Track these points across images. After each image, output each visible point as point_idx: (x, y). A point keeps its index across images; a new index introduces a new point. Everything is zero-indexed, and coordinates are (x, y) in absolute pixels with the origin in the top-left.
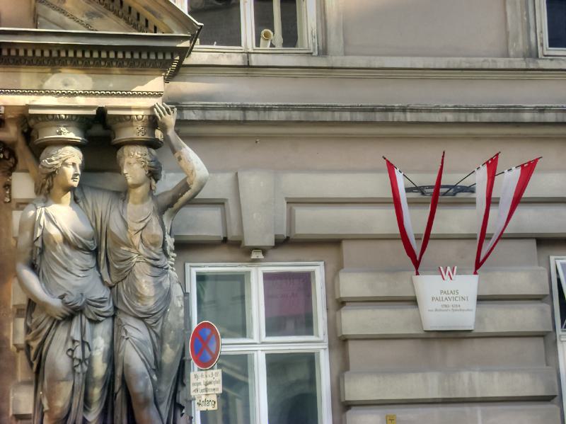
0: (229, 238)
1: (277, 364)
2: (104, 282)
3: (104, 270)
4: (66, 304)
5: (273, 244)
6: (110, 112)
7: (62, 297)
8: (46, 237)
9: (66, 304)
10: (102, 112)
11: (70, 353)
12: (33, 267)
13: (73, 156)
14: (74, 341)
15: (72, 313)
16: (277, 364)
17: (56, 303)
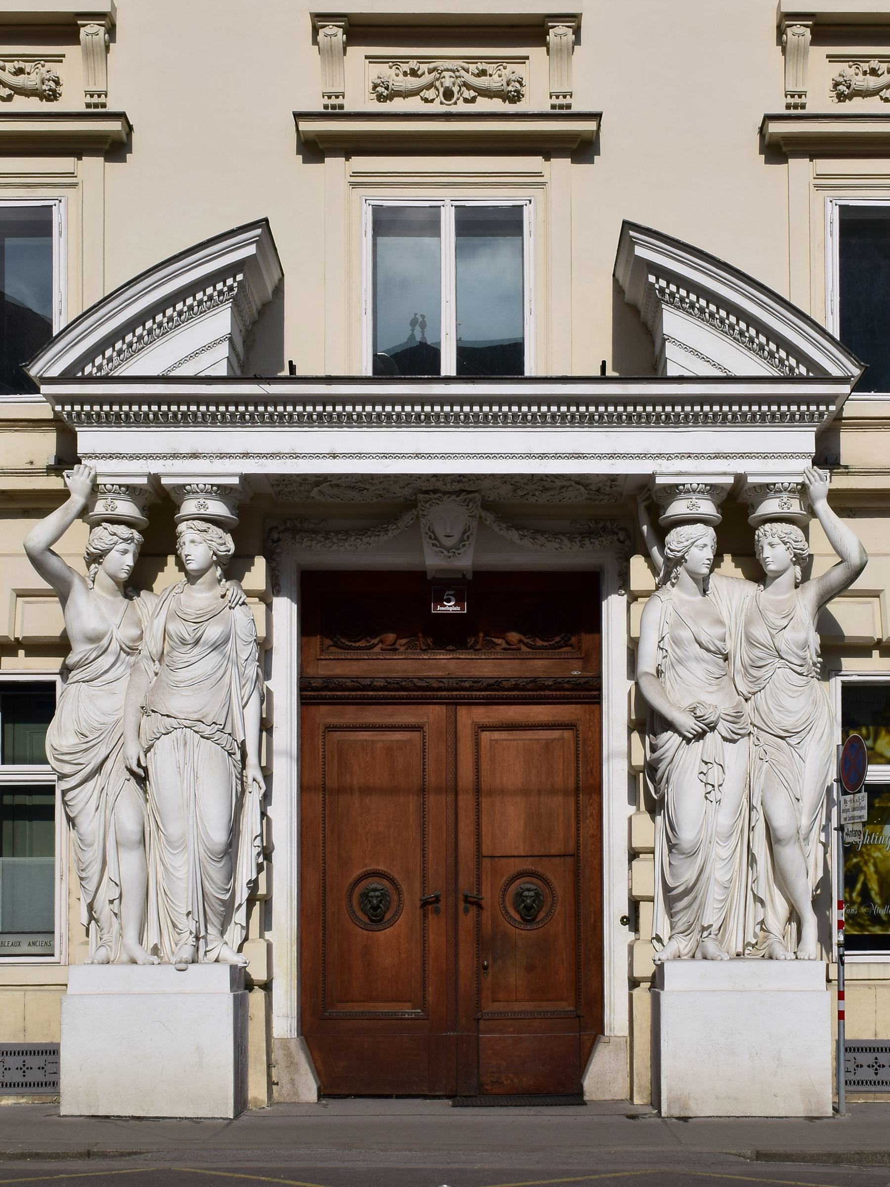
6: (750, 480)
10: (740, 478)
11: (702, 776)
13: (706, 535)
14: (706, 763)
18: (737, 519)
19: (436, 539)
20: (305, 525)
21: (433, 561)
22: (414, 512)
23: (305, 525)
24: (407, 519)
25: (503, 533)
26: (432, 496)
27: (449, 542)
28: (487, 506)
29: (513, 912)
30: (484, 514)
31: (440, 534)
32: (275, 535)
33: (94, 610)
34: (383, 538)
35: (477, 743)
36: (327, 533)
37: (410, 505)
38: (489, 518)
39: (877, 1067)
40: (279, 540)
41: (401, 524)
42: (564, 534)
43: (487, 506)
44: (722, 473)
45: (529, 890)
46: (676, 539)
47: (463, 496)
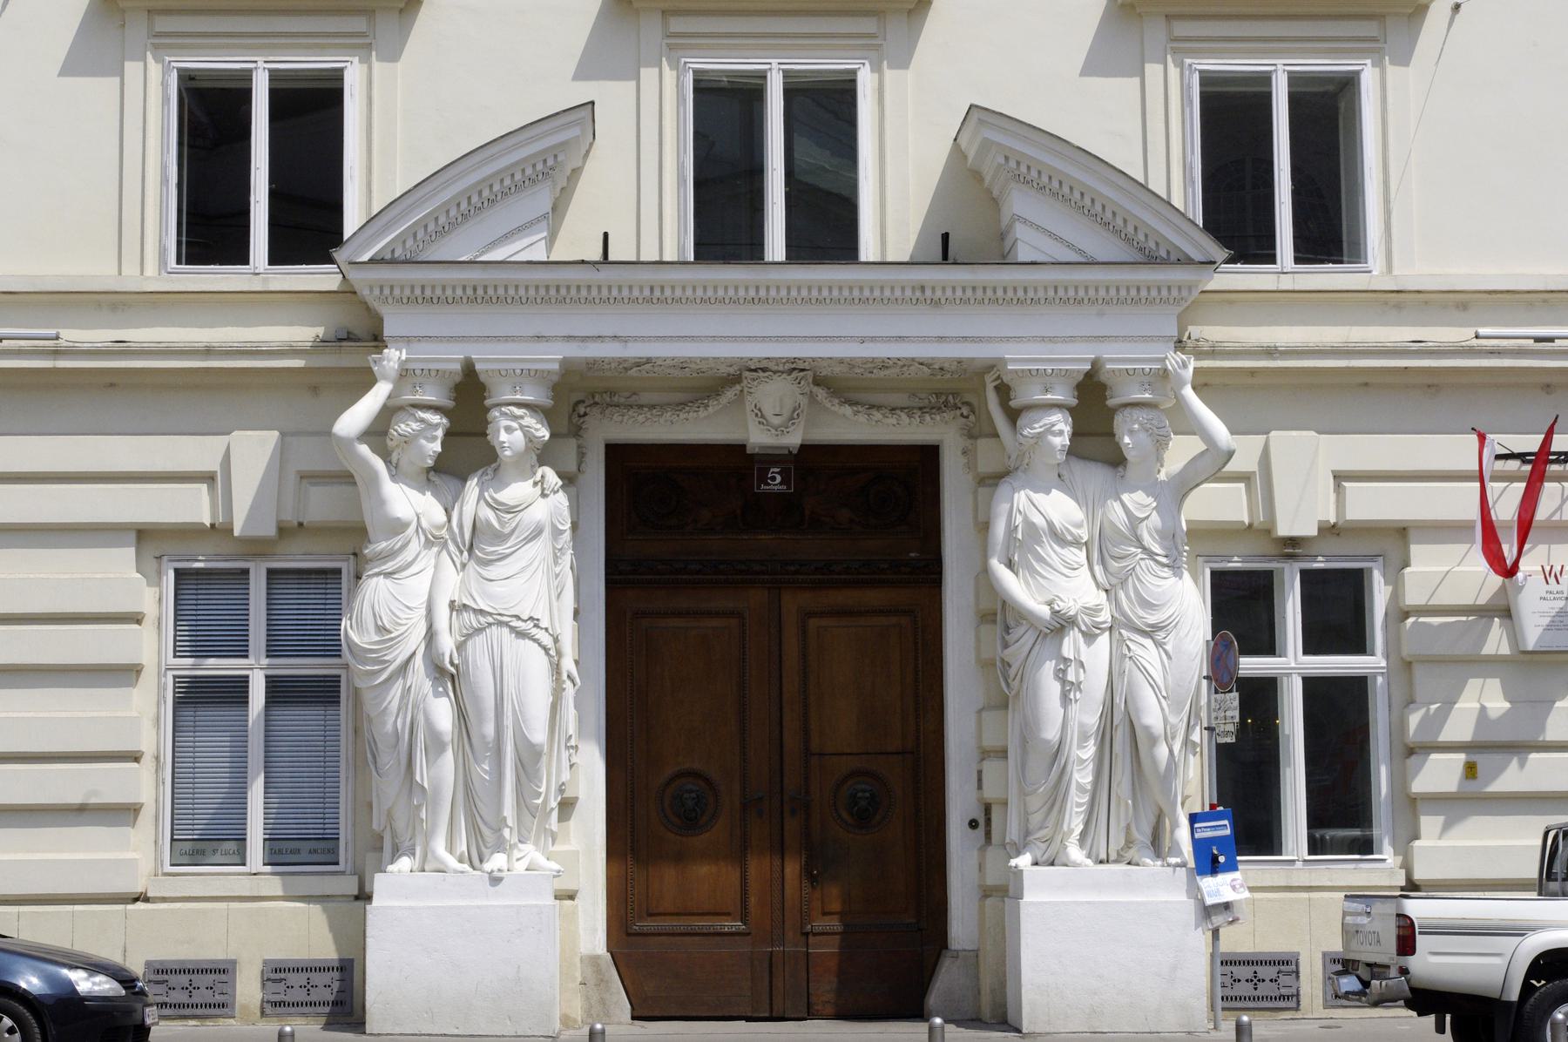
0: (1256, 524)
1: (1315, 687)
2: (1098, 585)
3: (1098, 569)
4: (1055, 613)
5: (1315, 533)
7: (1050, 604)
8: (1030, 526)
9: (1055, 613)
12: (1010, 565)
15: (1061, 625)
16: (1315, 687)
17: (1045, 611)
18: (1095, 409)
19: (763, 416)
20: (616, 399)
21: (758, 438)
22: (738, 387)
23: (616, 399)
24: (730, 394)
25: (836, 408)
26: (761, 374)
27: (776, 421)
28: (818, 382)
29: (845, 815)
30: (815, 389)
31: (768, 411)
32: (582, 410)
33: (406, 501)
34: (702, 413)
35: (804, 631)
36: (641, 407)
37: (735, 379)
38: (821, 393)
39: (1255, 981)
40: (585, 414)
41: (724, 400)
42: (902, 409)
43: (818, 382)
44: (1078, 358)
45: (864, 791)
46: (1032, 427)
47: (795, 374)
